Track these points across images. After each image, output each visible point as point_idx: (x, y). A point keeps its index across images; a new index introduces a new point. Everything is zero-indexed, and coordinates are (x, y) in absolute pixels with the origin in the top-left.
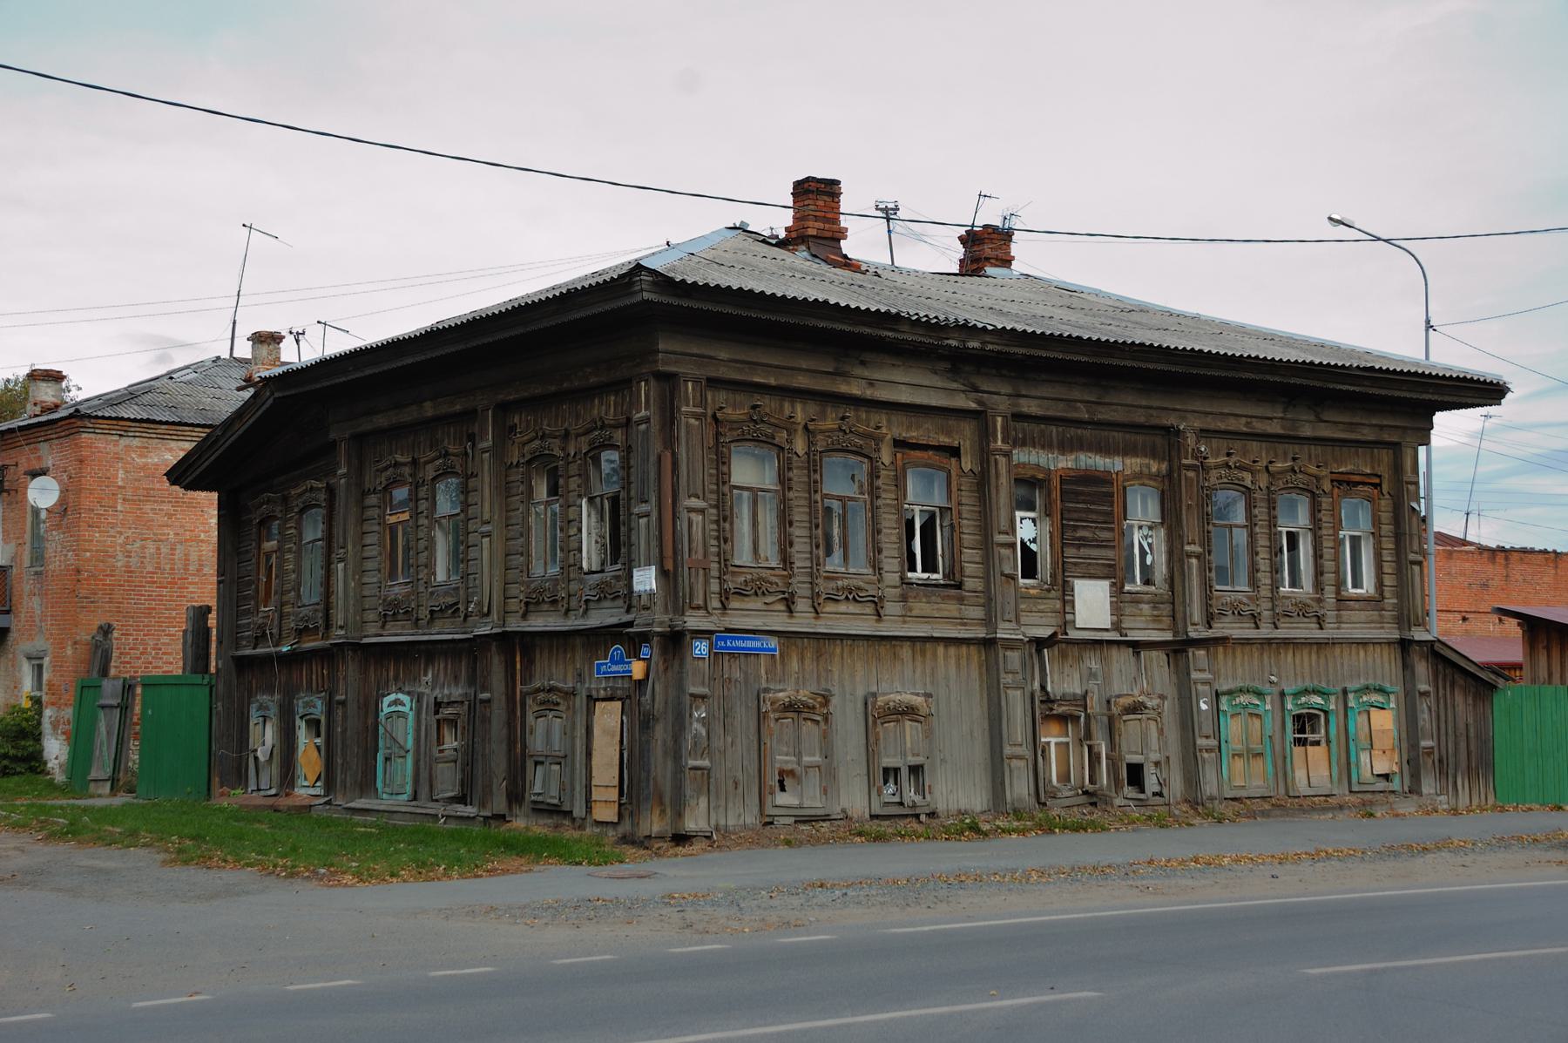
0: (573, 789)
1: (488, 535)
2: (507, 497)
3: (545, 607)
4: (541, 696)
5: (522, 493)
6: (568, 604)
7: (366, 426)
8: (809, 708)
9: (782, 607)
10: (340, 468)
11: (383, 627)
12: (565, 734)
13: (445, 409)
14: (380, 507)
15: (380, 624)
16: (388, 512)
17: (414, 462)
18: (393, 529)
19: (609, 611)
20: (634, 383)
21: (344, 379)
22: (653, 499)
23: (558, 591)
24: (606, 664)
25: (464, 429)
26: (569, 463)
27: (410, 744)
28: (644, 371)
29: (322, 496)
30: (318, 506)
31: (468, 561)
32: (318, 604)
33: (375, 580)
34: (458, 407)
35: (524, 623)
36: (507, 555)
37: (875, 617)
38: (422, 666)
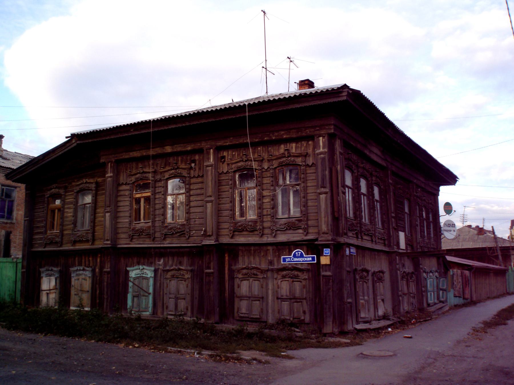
0: (267, 312)
1: (211, 201)
2: (219, 186)
3: (245, 233)
4: (245, 271)
5: (231, 184)
6: (154, 235)
7: (219, 144)
8: (295, 276)
9: (355, 236)
10: (108, 173)
11: (131, 241)
12: (262, 287)
13: (179, 148)
14: (130, 190)
15: (130, 239)
16: (134, 192)
17: (155, 172)
18: (138, 201)
19: (292, 235)
20: (316, 138)
21: (126, 135)
22: (328, 185)
23: (257, 226)
24: (290, 258)
25: (189, 158)
26: (263, 172)
27: (151, 290)
28: (323, 133)
29: (94, 185)
30: (91, 190)
31: (190, 213)
32: (89, 230)
33: (127, 220)
34: (189, 148)
35: (232, 240)
36: (219, 211)
37: (371, 242)
38: (204, 257)
